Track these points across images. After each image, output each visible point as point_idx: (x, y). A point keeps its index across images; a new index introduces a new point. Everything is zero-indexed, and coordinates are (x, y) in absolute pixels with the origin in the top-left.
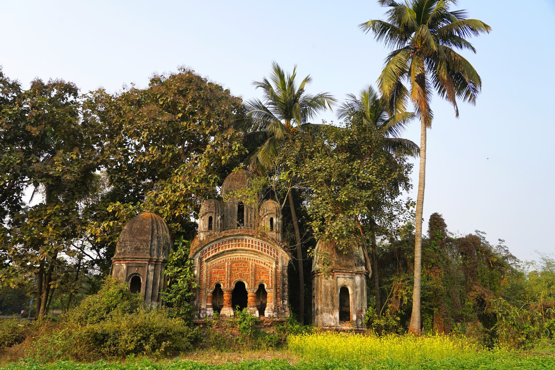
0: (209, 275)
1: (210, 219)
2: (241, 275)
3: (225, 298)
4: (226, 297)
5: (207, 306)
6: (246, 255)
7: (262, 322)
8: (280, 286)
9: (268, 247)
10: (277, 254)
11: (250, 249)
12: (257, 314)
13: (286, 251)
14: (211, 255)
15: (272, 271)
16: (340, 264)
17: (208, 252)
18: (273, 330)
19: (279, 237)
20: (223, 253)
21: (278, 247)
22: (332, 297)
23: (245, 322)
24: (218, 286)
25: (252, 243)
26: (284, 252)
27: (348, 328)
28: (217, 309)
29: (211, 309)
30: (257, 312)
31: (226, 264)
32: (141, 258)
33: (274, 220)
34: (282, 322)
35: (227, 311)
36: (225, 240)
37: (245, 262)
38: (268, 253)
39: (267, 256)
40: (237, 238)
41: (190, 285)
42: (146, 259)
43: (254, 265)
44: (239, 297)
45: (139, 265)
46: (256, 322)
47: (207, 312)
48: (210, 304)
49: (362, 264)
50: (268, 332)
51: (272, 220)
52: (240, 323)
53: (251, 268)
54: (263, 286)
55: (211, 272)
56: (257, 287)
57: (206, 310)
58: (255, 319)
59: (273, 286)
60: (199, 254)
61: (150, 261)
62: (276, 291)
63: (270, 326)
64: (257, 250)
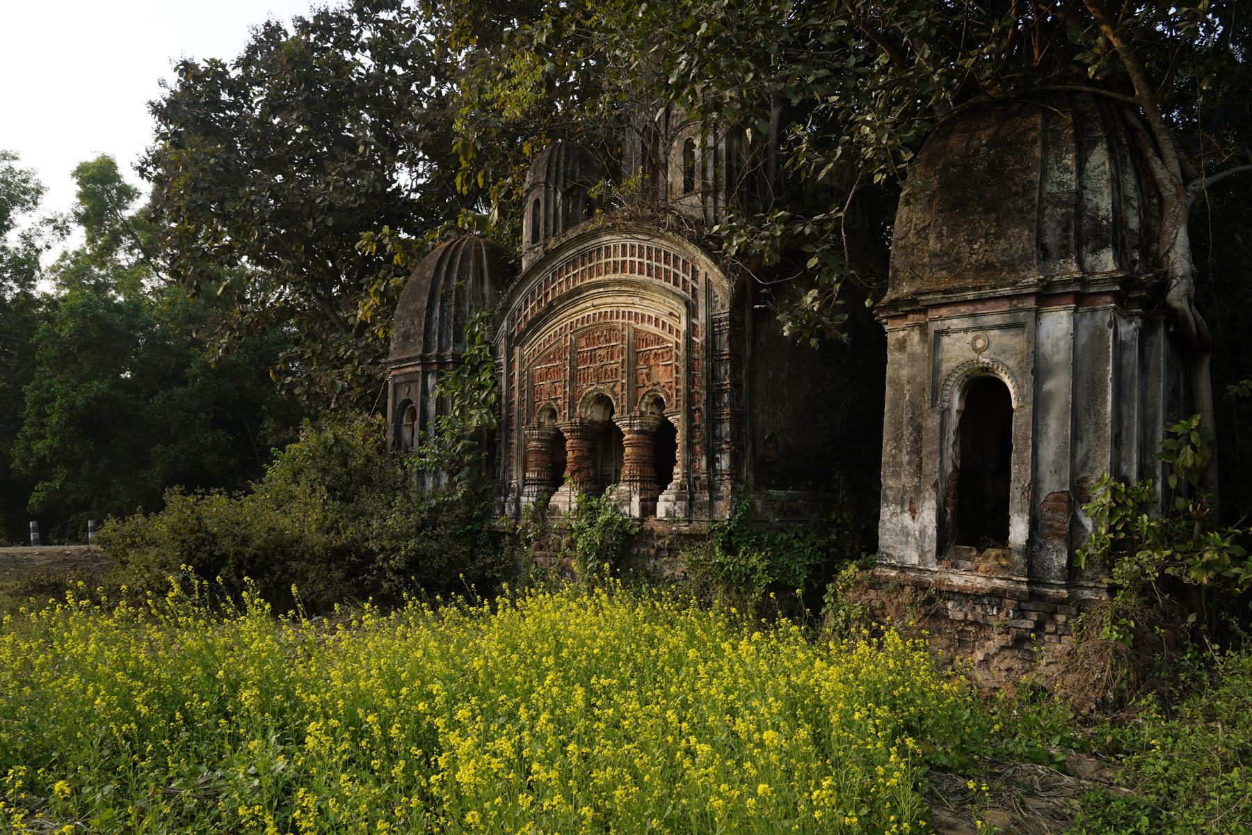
10: (694, 278)
32: (409, 360)
61: (425, 361)
64: (636, 276)
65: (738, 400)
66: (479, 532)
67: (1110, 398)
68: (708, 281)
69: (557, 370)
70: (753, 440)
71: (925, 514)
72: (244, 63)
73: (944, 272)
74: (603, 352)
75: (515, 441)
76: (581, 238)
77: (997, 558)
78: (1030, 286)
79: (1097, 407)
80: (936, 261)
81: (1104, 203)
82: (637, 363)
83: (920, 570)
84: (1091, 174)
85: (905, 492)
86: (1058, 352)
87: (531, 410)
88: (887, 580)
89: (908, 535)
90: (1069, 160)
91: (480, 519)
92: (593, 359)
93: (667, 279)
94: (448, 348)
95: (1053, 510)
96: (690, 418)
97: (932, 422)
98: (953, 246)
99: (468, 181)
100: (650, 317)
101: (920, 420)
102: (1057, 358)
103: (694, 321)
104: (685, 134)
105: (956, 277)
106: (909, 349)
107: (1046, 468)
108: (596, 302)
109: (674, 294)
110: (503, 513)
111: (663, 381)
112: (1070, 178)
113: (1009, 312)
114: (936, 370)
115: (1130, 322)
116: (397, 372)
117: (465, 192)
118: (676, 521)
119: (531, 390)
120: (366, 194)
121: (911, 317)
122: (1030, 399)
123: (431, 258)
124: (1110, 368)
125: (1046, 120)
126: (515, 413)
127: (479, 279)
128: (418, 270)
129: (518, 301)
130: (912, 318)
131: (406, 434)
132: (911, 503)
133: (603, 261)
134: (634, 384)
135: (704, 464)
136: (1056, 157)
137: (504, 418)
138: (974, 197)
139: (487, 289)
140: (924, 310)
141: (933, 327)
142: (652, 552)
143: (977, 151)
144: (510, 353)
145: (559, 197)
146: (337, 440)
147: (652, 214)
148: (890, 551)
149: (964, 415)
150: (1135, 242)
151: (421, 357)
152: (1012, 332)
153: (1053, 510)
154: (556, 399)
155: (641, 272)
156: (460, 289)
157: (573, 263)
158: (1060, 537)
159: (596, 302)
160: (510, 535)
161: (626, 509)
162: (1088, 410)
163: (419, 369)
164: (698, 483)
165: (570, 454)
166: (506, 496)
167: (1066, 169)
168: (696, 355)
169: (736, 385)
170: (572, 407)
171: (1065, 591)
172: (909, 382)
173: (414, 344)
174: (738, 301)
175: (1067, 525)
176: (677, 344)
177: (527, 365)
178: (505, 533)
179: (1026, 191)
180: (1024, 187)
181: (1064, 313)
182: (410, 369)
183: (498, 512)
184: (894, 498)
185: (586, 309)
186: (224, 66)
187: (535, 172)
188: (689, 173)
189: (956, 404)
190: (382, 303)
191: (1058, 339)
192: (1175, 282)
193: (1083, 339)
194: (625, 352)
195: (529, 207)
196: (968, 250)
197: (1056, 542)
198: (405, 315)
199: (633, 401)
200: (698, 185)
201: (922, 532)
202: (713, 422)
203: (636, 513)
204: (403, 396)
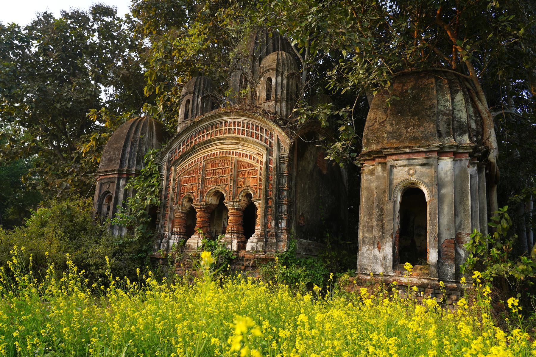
16: (398, 137)
22: (381, 210)
25: (235, 125)
27: (415, 280)
36: (198, 128)
39: (254, 143)
42: (114, 171)
45: (109, 180)
49: (462, 129)
61: (120, 173)
64: (240, 136)
65: (290, 195)
66: (145, 258)
67: (470, 197)
68: (278, 139)
69: (194, 179)
70: (296, 214)
71: (386, 249)
72: (30, 28)
73: (394, 140)
74: (220, 171)
75: (169, 212)
76: (212, 117)
77: (421, 269)
78: (436, 147)
79: (464, 202)
80: (390, 135)
81: (463, 116)
82: (238, 176)
83: (384, 275)
84: (457, 104)
85: (375, 239)
86: (447, 177)
88: (366, 281)
89: (377, 259)
90: (448, 97)
91: (146, 251)
92: (214, 173)
93: (257, 138)
94: (133, 167)
95: (447, 247)
96: (266, 202)
97: (389, 206)
98: (398, 129)
99: (150, 90)
100: (246, 155)
101: (382, 206)
102: (446, 179)
103: (270, 157)
104: (268, 75)
105: (400, 142)
106: (376, 174)
107: (443, 229)
108: (218, 147)
109: (261, 144)
110: (159, 248)
111: (252, 185)
112: (449, 104)
113: (425, 158)
114: (391, 183)
115: (474, 167)
116: (103, 177)
117: (148, 96)
118: (257, 252)
119: (179, 188)
120: (90, 95)
121: (377, 159)
122: (436, 196)
123: (127, 124)
124: (469, 185)
125: (436, 81)
126: (170, 199)
127: (151, 136)
128: (119, 129)
129: (175, 145)
130: (378, 160)
131: (105, 209)
132: (378, 244)
133: (223, 128)
134: (236, 186)
135: (273, 224)
136: (442, 95)
137: (163, 201)
138: (409, 108)
139: (155, 141)
140: (385, 157)
141: (389, 164)
142: (243, 268)
143: (407, 91)
144: (169, 169)
145: (199, 100)
146: (68, 208)
147: (249, 108)
148: (367, 267)
149: (402, 204)
150: (475, 133)
151: (118, 170)
152: (426, 167)
153: (447, 247)
154: (193, 192)
155: (243, 134)
156: (141, 139)
157: (207, 128)
158: (451, 259)
159: (218, 147)
160: (163, 259)
161: (230, 246)
162: (460, 203)
163: (116, 176)
164: (269, 234)
165: (198, 220)
166: (162, 240)
167: (447, 101)
168: (270, 173)
169: (290, 188)
170: (202, 196)
171: (455, 285)
172: (376, 189)
173: (114, 164)
174: (292, 149)
175: (454, 254)
176: (261, 168)
177: (178, 175)
178: (160, 258)
179: (431, 108)
180: (430, 106)
181: (449, 160)
182: (111, 176)
183: (156, 248)
184: (368, 242)
185: (213, 150)
186: (19, 27)
187: (188, 87)
188: (269, 91)
189: (399, 199)
190: (96, 144)
191: (447, 171)
192: (492, 151)
193: (457, 172)
194: (233, 171)
195: (184, 103)
196: (405, 131)
197: (449, 262)
198: (110, 150)
199: (236, 194)
200: (273, 97)
201: (385, 258)
202: (279, 204)
203: (235, 248)
204: (105, 189)
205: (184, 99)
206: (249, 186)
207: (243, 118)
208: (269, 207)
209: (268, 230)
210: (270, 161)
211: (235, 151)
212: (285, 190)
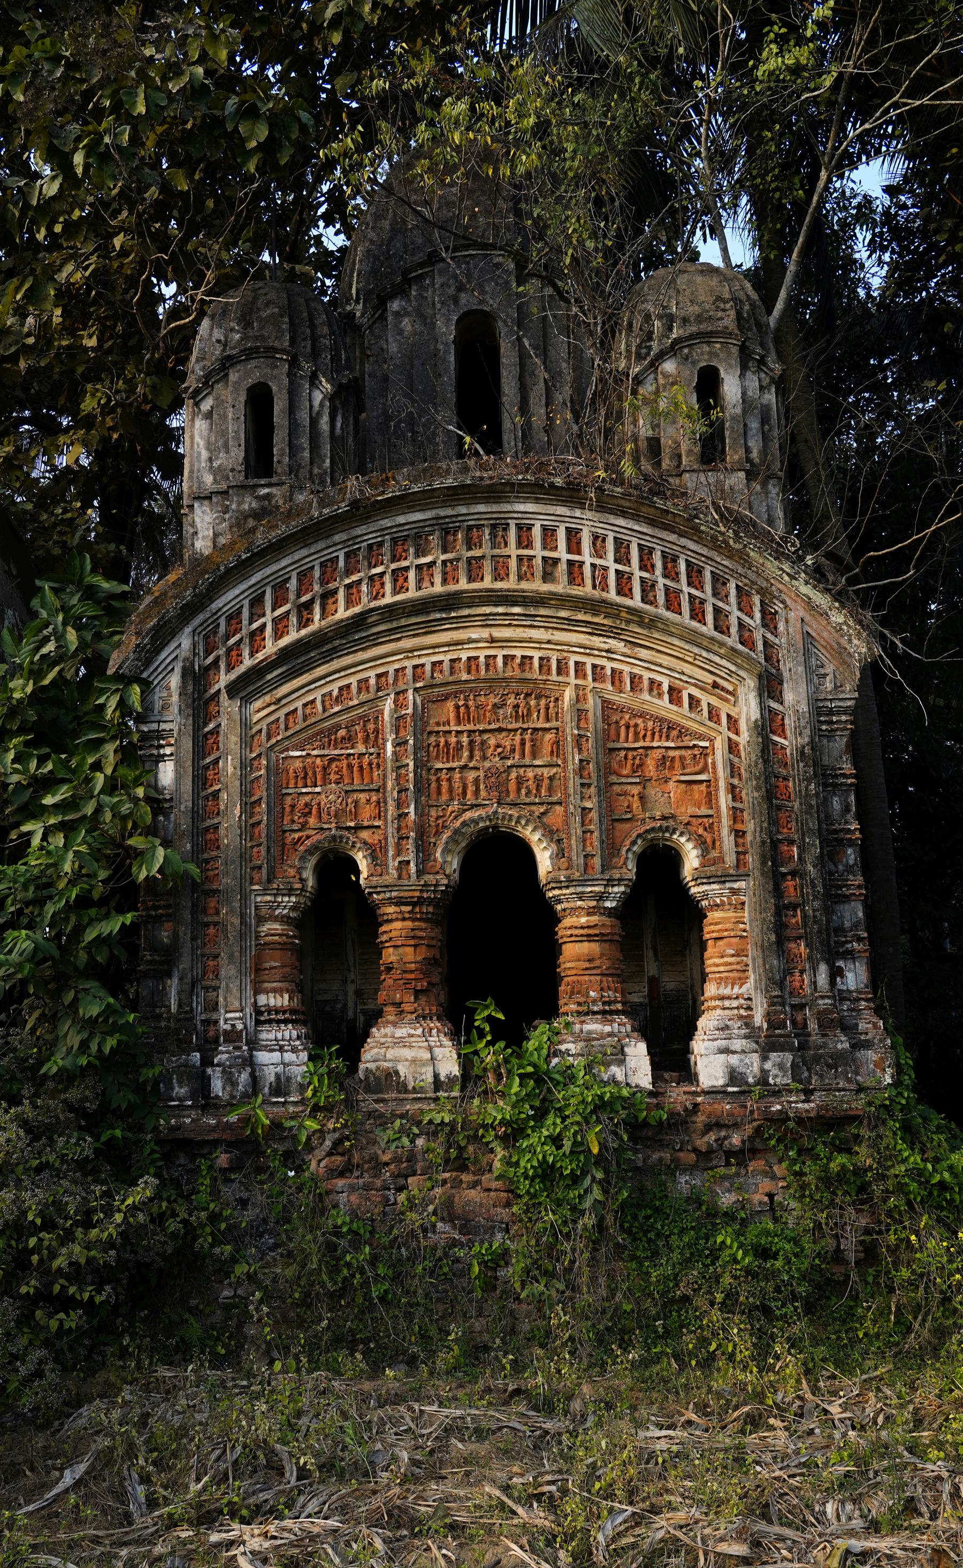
0: (261, 792)
1: (259, 402)
2: (498, 784)
3: (390, 956)
4: (401, 942)
5: (262, 1017)
6: (533, 640)
7: (680, 1122)
8: (803, 854)
9: (694, 574)
10: (769, 619)
11: (560, 587)
12: (638, 1065)
13: (839, 597)
14: (271, 647)
15: (732, 747)
17: (246, 628)
18: (766, 1185)
19: (771, 504)
20: (354, 632)
21: (772, 566)
23: (552, 1125)
24: (336, 867)
26: (821, 600)
28: (338, 1032)
29: (289, 1032)
30: (638, 1055)
31: (388, 706)
33: (731, 388)
34: (834, 1126)
35: (412, 1050)
36: (366, 533)
37: (529, 688)
38: (697, 614)
39: (693, 638)
40: (456, 516)
41: (121, 859)
43: (591, 703)
44: (493, 947)
46: (636, 1128)
47: (263, 1057)
48: (282, 1001)
50: (727, 1200)
51: (708, 385)
52: (513, 1133)
53: (570, 731)
54: (674, 858)
55: (275, 771)
56: (630, 870)
57: (254, 1044)
58: (628, 1103)
59: (751, 860)
60: (185, 641)
62: (778, 892)
63: (741, 1156)
87: (275, 850)
103: (774, 705)
108: (498, 633)
159: (498, 633)
178: (215, 1143)
205: (233, 376)
206: (673, 817)
207: (621, 522)
208: (787, 907)
209: (795, 1001)
210: (772, 720)
211: (589, 661)
212: (851, 843)
